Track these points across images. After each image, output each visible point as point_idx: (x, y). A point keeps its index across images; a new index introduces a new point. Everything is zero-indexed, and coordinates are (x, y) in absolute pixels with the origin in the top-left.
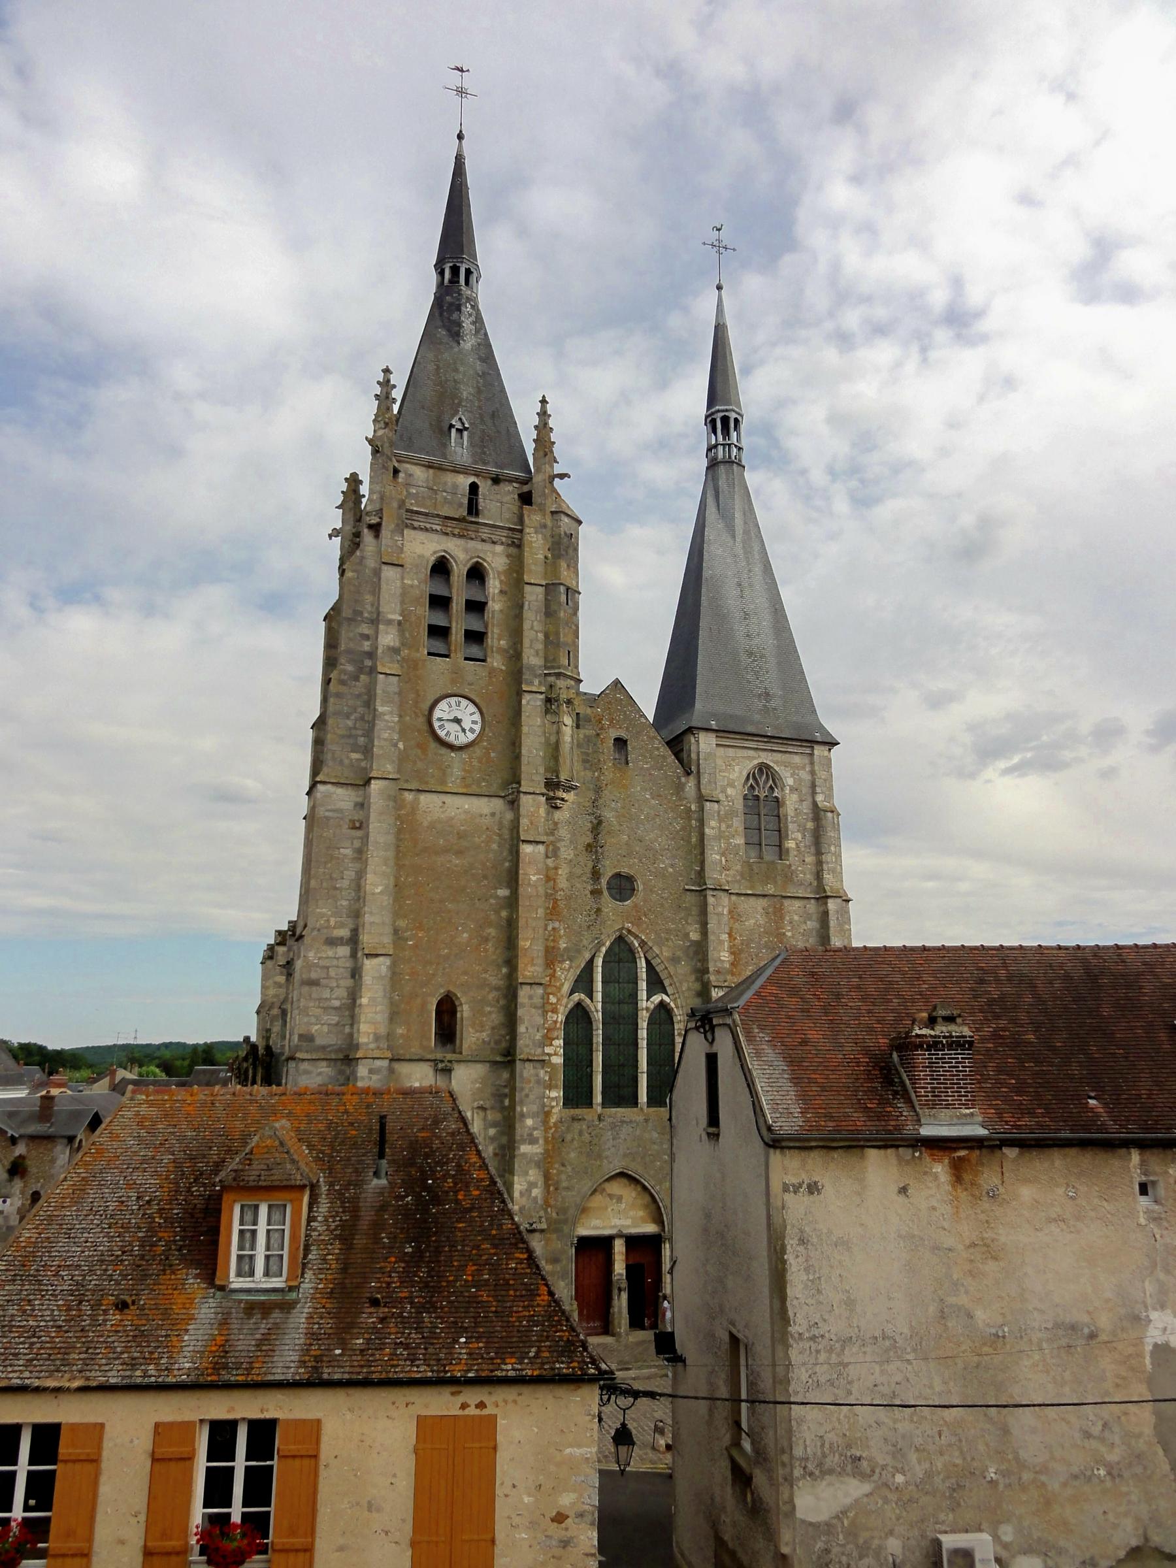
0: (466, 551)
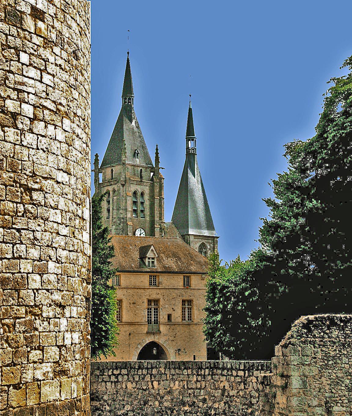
0: (141, 189)
